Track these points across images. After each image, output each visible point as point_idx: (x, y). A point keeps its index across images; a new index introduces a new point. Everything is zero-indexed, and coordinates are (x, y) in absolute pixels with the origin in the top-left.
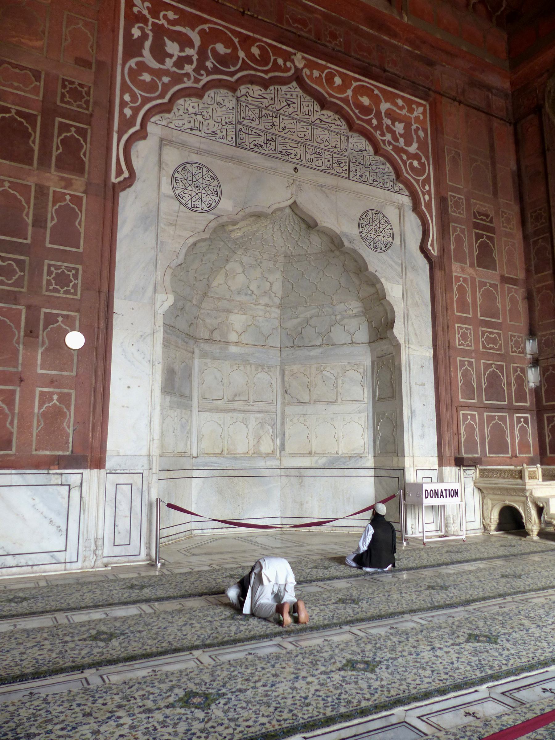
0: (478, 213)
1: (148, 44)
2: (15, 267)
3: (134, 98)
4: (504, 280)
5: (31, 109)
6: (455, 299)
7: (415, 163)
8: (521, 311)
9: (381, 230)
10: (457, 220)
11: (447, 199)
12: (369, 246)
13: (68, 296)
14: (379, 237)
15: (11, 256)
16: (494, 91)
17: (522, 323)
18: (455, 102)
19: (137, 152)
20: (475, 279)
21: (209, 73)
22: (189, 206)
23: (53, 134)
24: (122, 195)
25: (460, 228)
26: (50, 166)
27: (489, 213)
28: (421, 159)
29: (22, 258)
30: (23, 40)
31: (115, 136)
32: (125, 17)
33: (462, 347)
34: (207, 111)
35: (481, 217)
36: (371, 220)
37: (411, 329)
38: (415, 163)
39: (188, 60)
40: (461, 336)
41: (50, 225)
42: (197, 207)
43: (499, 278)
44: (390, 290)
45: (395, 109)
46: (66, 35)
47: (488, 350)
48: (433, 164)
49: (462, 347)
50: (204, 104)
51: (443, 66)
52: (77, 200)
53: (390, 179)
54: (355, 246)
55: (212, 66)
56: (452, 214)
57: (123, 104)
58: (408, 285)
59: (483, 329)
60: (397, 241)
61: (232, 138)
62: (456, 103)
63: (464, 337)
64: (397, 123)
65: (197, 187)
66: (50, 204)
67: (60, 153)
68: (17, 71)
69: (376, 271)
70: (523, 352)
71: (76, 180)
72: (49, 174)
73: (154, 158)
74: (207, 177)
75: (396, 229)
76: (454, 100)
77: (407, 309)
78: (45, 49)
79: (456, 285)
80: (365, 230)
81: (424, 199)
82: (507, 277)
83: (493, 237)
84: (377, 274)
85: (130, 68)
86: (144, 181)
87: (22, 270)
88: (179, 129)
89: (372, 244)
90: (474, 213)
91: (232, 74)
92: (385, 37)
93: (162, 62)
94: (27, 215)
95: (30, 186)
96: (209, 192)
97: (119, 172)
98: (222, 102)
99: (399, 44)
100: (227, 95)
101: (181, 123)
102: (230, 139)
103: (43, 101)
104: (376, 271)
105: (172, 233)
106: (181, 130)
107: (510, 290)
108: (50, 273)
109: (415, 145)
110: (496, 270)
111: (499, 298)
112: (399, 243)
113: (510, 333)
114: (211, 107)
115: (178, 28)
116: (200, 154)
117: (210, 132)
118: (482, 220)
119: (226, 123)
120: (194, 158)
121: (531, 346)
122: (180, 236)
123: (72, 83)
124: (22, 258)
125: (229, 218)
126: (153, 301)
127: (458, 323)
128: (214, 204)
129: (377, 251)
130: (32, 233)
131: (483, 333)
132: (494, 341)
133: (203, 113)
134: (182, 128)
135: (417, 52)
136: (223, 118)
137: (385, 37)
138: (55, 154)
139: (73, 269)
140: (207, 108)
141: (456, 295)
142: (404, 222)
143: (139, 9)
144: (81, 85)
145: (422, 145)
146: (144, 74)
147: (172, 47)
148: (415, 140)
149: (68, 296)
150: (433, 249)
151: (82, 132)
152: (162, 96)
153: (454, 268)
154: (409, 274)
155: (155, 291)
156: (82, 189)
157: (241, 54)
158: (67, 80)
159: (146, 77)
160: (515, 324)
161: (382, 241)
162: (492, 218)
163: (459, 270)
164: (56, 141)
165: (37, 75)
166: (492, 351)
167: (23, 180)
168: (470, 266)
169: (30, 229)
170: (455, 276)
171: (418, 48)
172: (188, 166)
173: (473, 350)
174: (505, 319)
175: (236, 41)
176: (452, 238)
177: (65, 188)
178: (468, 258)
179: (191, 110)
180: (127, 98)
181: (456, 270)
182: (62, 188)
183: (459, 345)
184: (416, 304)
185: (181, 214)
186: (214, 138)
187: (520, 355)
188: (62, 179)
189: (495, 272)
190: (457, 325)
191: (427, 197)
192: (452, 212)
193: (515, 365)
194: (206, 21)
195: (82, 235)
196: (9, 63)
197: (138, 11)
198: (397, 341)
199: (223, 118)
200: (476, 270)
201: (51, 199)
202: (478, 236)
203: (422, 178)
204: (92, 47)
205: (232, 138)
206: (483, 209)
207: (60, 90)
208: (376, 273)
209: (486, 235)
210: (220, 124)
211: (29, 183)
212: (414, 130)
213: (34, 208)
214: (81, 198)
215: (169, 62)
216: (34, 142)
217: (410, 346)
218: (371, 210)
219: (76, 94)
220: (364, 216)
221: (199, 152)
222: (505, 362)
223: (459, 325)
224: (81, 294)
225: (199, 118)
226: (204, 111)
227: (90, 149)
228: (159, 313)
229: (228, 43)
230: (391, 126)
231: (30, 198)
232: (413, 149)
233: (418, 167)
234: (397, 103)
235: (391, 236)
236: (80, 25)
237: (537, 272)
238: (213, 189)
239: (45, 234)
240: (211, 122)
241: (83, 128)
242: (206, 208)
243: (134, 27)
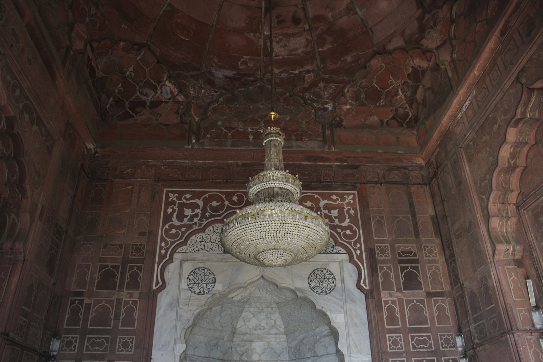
0: (402, 252)
1: (175, 215)
2: (105, 342)
3: (166, 243)
4: (429, 295)
5: (118, 263)
6: (385, 317)
7: (348, 232)
8: (449, 315)
9: (326, 280)
10: (384, 262)
11: (374, 249)
12: (316, 293)
13: (128, 353)
14: (324, 285)
15: (103, 336)
16: (410, 168)
17: (451, 324)
18: (378, 185)
19: (169, 270)
20: (403, 299)
21: (207, 219)
22: (197, 292)
23: (126, 272)
24: (159, 295)
25: (386, 266)
26: (123, 289)
27: (412, 250)
28: (353, 228)
29: (108, 336)
30: (116, 232)
31: (156, 265)
32: (164, 205)
33: (393, 351)
34: (208, 238)
35: (405, 254)
36: (318, 275)
37: (351, 343)
38: (348, 232)
39: (196, 215)
40: (392, 343)
41: (121, 317)
42: (201, 292)
43: (425, 294)
44: (334, 319)
45: (331, 202)
46: (135, 224)
47: (418, 350)
48: (362, 229)
49: (393, 351)
50: (206, 235)
51: (366, 165)
52: (135, 303)
53: (331, 246)
54: (305, 294)
55: (209, 214)
56: (379, 258)
57: (161, 248)
58: (348, 313)
59: (412, 334)
60: (339, 285)
61: (222, 249)
62: (379, 185)
63: (395, 343)
64: (332, 211)
65: (201, 281)
66: (122, 307)
67: (129, 281)
68: (113, 247)
69: (322, 308)
70: (454, 345)
71: (135, 292)
72: (123, 292)
73: (177, 271)
74: (207, 274)
75: (338, 277)
76: (376, 183)
77: (348, 330)
78: (126, 234)
79: (385, 306)
80: (313, 282)
81: (356, 254)
82: (432, 292)
83: (418, 267)
84: (323, 309)
85: (166, 229)
86: (172, 284)
87: (107, 342)
88: (191, 252)
89: (319, 290)
90: (399, 253)
91: (220, 215)
92: (320, 163)
93: (182, 221)
94: (112, 315)
95: (114, 300)
96: (208, 282)
97: (157, 283)
98: (216, 231)
99: (331, 163)
100: (219, 226)
101: (192, 249)
102: (221, 250)
103: (123, 258)
104: (322, 308)
105: (186, 309)
106: (193, 253)
107: (436, 302)
108: (120, 342)
109: (347, 220)
110: (422, 289)
111: (426, 309)
112: (340, 285)
113: (439, 334)
114: (210, 235)
115: (192, 201)
116: (204, 262)
117: (209, 249)
118: (406, 256)
119: (218, 242)
120: (201, 265)
121: (459, 341)
122: (191, 310)
123: (136, 245)
124: (108, 336)
125: (219, 295)
126: (174, 349)
127: (388, 333)
128: (211, 288)
129: (323, 295)
130: (113, 323)
131: (413, 338)
132: (424, 342)
133: (205, 240)
134: (193, 251)
135: (344, 164)
136: (217, 239)
137: (320, 163)
138: (126, 282)
139: (131, 338)
140: (208, 237)
141: (386, 314)
142: (343, 272)
143: (172, 199)
144: (140, 245)
145: (353, 219)
146: (172, 230)
147: (188, 212)
148: (347, 217)
149: (128, 353)
150: (366, 286)
151: (139, 268)
152: (181, 239)
153: (382, 295)
154: (348, 306)
155: (175, 343)
156: (138, 297)
157: (227, 203)
158: (134, 245)
159: (174, 231)
160: (444, 326)
161: (326, 287)
162: (415, 253)
163: (387, 295)
164: (128, 275)
165: (121, 246)
166: (422, 350)
167: (111, 298)
168: (397, 291)
169: (112, 321)
170: (384, 301)
171: (345, 161)
172: (197, 270)
173: (404, 352)
174: (433, 323)
175: (224, 197)
176: (380, 275)
177: (130, 298)
178: (395, 285)
179: (199, 240)
180: (163, 244)
181: (385, 296)
182: (128, 298)
183: (390, 349)
184: (356, 325)
185: (192, 298)
186: (211, 252)
187: (450, 349)
188: (128, 293)
189: (421, 291)
190: (387, 335)
191: (358, 252)
192: (379, 257)
193: (447, 358)
194: (206, 193)
195: (136, 320)
196: (110, 244)
197: (172, 200)
198: (342, 353)
199: (217, 240)
200: (402, 293)
201: (123, 304)
202: (403, 269)
203: (353, 240)
204: (147, 225)
205: (222, 249)
206: (406, 248)
207: (131, 250)
208: (322, 309)
209: (410, 266)
210: (215, 243)
211: (114, 299)
212: (346, 211)
213: (115, 311)
214: (136, 301)
215: (186, 220)
216: (117, 279)
217: (352, 355)
218: (318, 269)
219: (138, 250)
220: (313, 274)
221: (202, 261)
222: (436, 356)
223: (390, 335)
224: (134, 351)
225: (203, 243)
226: (206, 238)
227: (143, 275)
228: (177, 355)
229: (219, 199)
230: (328, 214)
231: (113, 307)
232: (346, 223)
233: (351, 233)
234: (332, 198)
235: (334, 282)
236: (142, 217)
237: (455, 285)
238: (210, 280)
239: (119, 322)
240: (210, 244)
241: (140, 266)
242: (206, 292)
243: (168, 208)
